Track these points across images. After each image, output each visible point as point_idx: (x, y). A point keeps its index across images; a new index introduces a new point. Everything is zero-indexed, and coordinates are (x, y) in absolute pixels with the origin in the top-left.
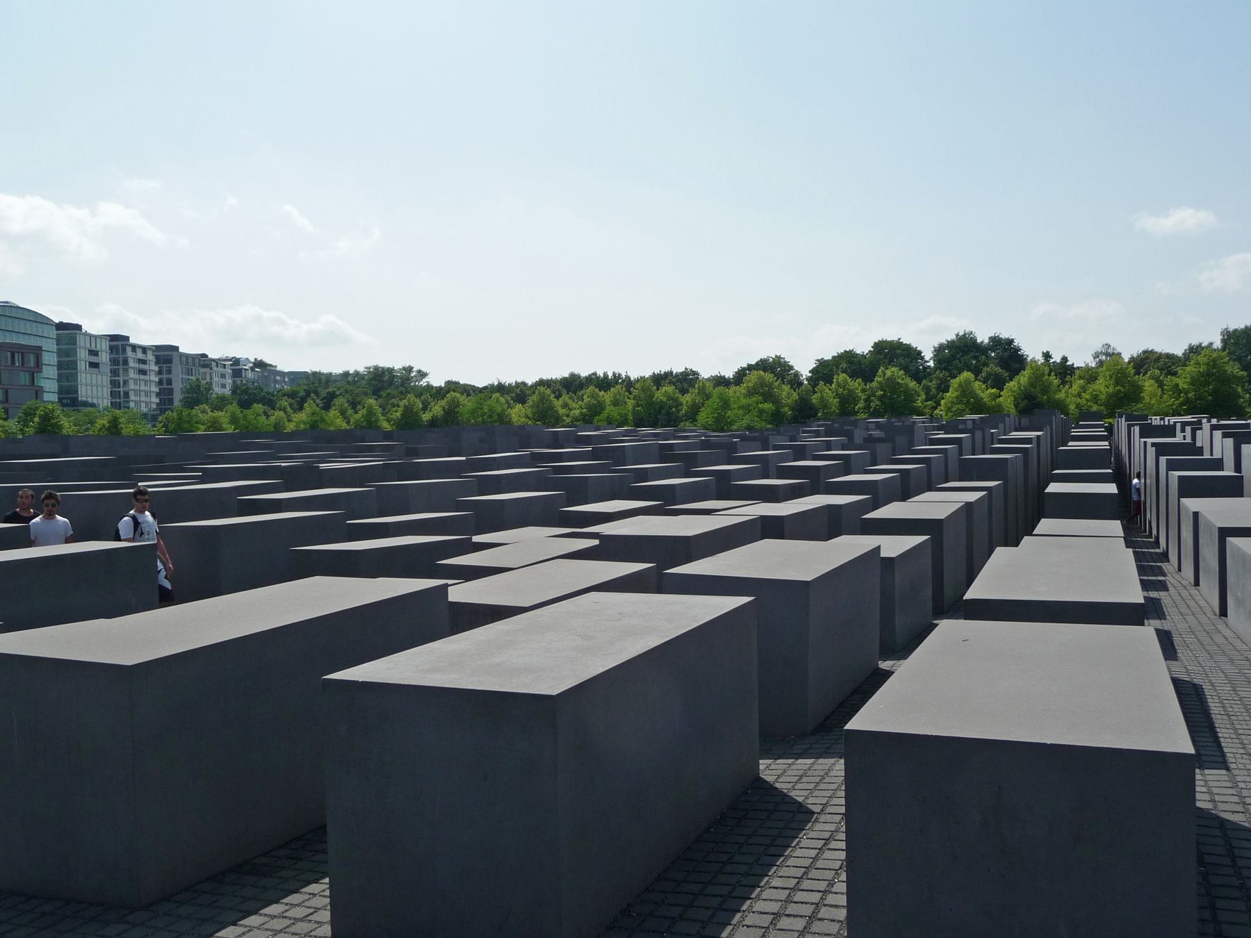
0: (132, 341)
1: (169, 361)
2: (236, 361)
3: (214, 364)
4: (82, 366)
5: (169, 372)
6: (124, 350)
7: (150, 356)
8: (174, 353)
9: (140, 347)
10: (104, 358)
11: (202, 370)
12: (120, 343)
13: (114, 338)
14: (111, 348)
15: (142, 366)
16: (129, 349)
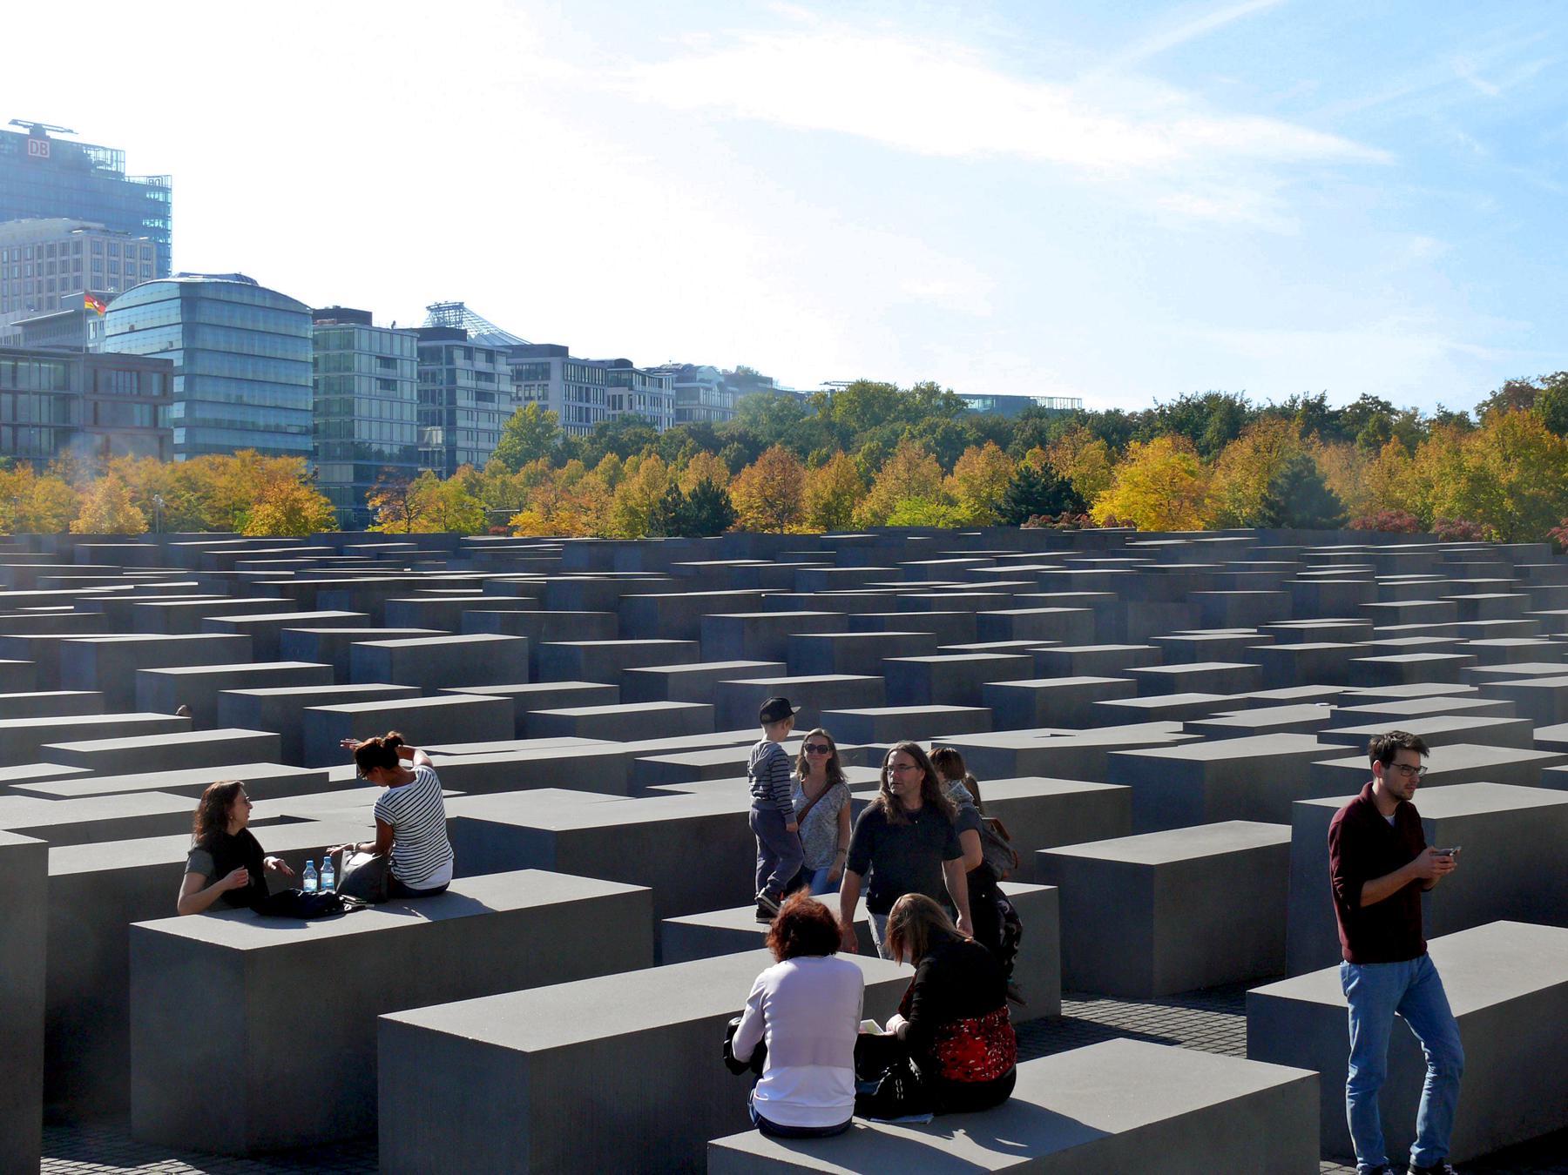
3: (636, 379)
4: (364, 386)
6: (451, 360)
7: (503, 367)
8: (556, 361)
10: (408, 370)
11: (612, 391)
12: (443, 343)
14: (421, 352)
15: (484, 385)
16: (459, 356)
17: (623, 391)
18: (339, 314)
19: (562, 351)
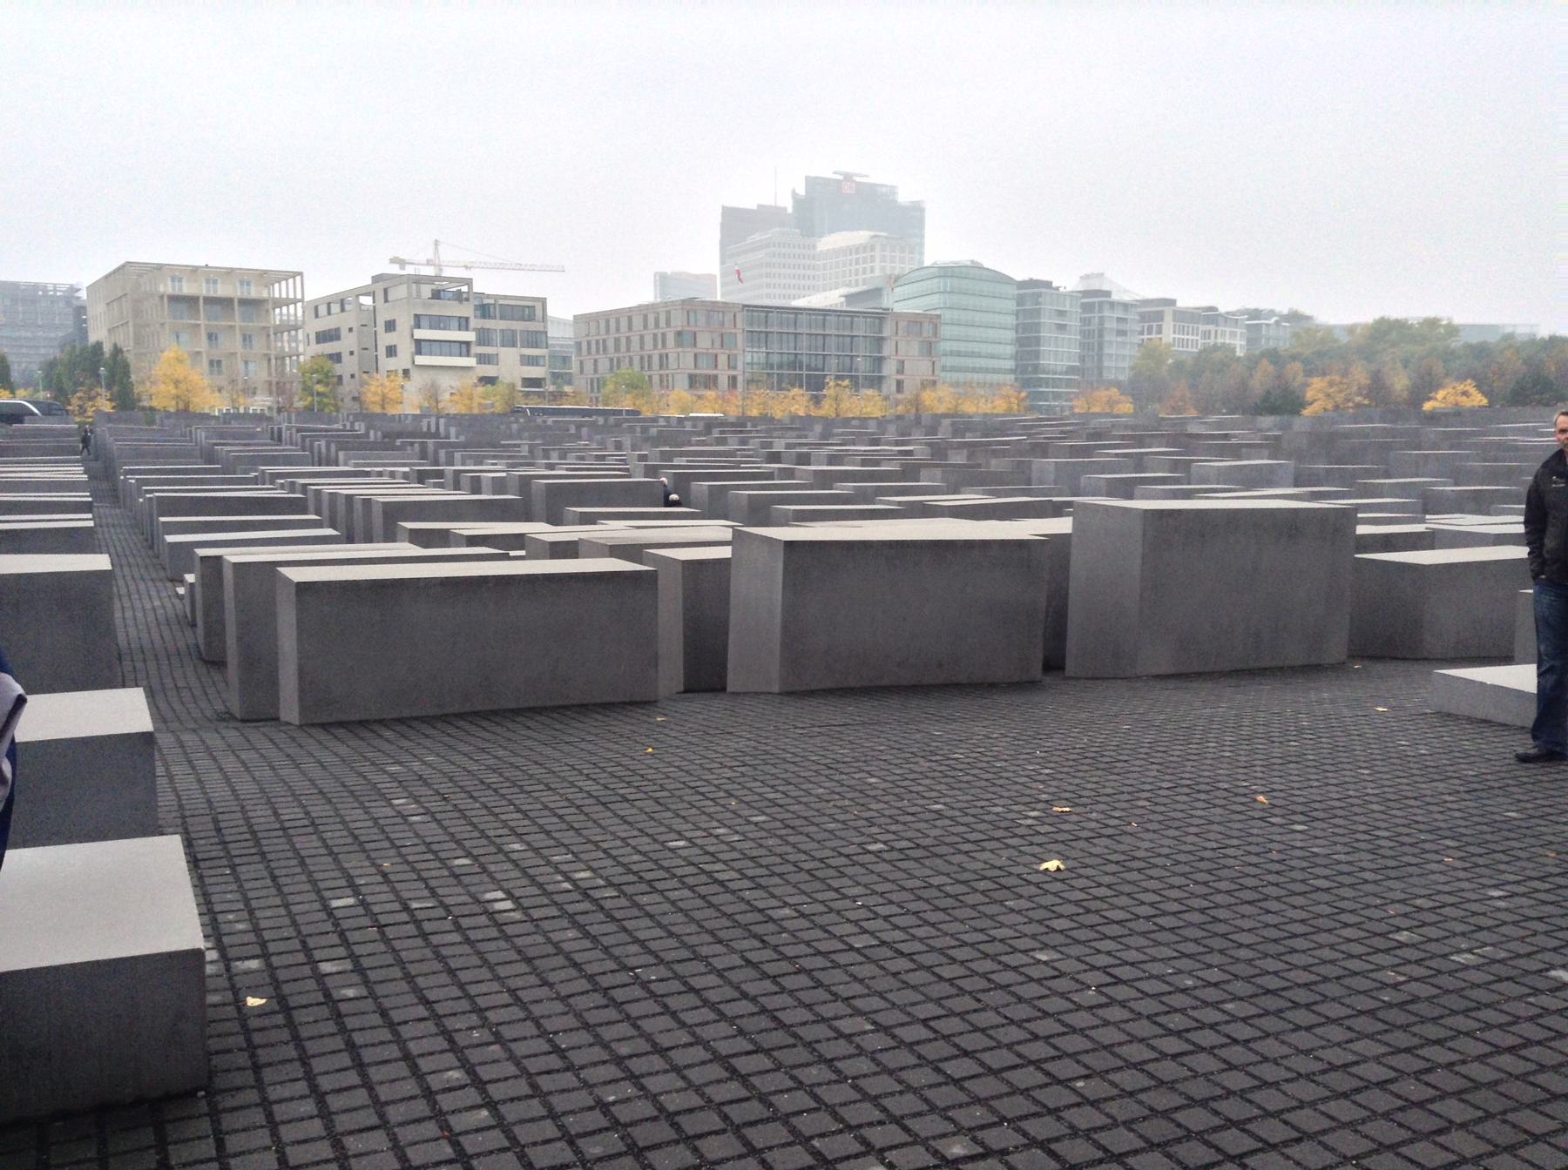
0: (1115, 297)
1: (1159, 316)
2: (1255, 314)
5: (1159, 332)
6: (1100, 311)
9: (1119, 303)
11: (1202, 328)
13: (1086, 293)
15: (1122, 327)
17: (1212, 327)
18: (1032, 283)
19: (1172, 302)
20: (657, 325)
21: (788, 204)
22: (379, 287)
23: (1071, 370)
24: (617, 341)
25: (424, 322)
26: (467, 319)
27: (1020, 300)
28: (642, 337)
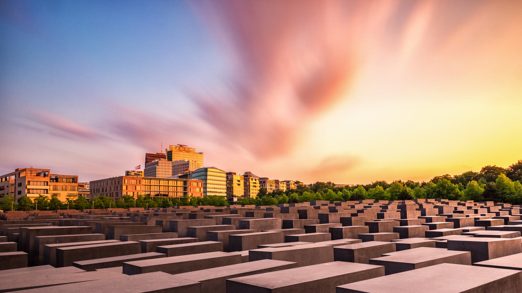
15: (255, 185)
20: (115, 184)
21: (164, 152)
22: (18, 172)
23: (242, 196)
24: (103, 189)
25: (31, 183)
26: (47, 182)
27: (227, 178)
28: (110, 187)
